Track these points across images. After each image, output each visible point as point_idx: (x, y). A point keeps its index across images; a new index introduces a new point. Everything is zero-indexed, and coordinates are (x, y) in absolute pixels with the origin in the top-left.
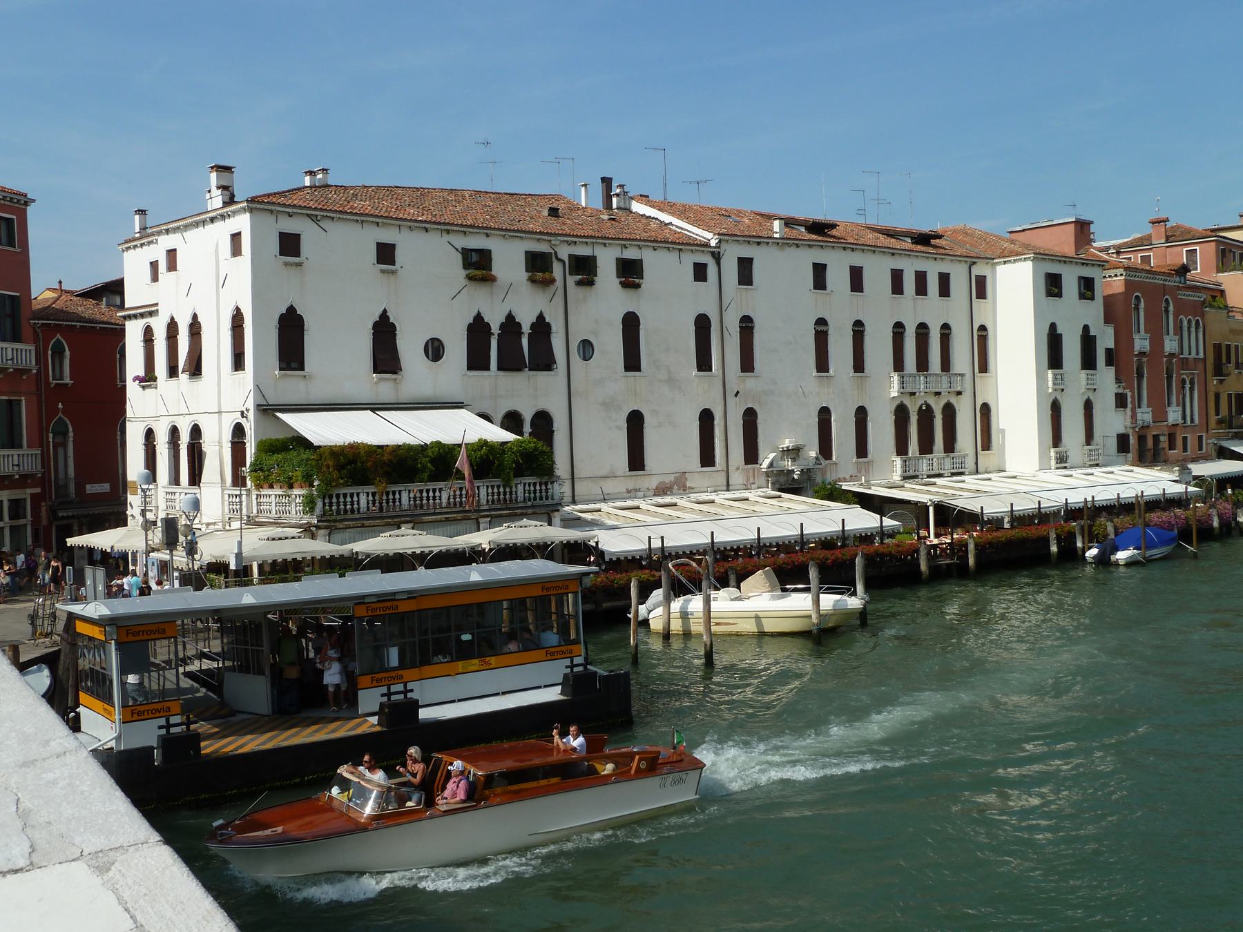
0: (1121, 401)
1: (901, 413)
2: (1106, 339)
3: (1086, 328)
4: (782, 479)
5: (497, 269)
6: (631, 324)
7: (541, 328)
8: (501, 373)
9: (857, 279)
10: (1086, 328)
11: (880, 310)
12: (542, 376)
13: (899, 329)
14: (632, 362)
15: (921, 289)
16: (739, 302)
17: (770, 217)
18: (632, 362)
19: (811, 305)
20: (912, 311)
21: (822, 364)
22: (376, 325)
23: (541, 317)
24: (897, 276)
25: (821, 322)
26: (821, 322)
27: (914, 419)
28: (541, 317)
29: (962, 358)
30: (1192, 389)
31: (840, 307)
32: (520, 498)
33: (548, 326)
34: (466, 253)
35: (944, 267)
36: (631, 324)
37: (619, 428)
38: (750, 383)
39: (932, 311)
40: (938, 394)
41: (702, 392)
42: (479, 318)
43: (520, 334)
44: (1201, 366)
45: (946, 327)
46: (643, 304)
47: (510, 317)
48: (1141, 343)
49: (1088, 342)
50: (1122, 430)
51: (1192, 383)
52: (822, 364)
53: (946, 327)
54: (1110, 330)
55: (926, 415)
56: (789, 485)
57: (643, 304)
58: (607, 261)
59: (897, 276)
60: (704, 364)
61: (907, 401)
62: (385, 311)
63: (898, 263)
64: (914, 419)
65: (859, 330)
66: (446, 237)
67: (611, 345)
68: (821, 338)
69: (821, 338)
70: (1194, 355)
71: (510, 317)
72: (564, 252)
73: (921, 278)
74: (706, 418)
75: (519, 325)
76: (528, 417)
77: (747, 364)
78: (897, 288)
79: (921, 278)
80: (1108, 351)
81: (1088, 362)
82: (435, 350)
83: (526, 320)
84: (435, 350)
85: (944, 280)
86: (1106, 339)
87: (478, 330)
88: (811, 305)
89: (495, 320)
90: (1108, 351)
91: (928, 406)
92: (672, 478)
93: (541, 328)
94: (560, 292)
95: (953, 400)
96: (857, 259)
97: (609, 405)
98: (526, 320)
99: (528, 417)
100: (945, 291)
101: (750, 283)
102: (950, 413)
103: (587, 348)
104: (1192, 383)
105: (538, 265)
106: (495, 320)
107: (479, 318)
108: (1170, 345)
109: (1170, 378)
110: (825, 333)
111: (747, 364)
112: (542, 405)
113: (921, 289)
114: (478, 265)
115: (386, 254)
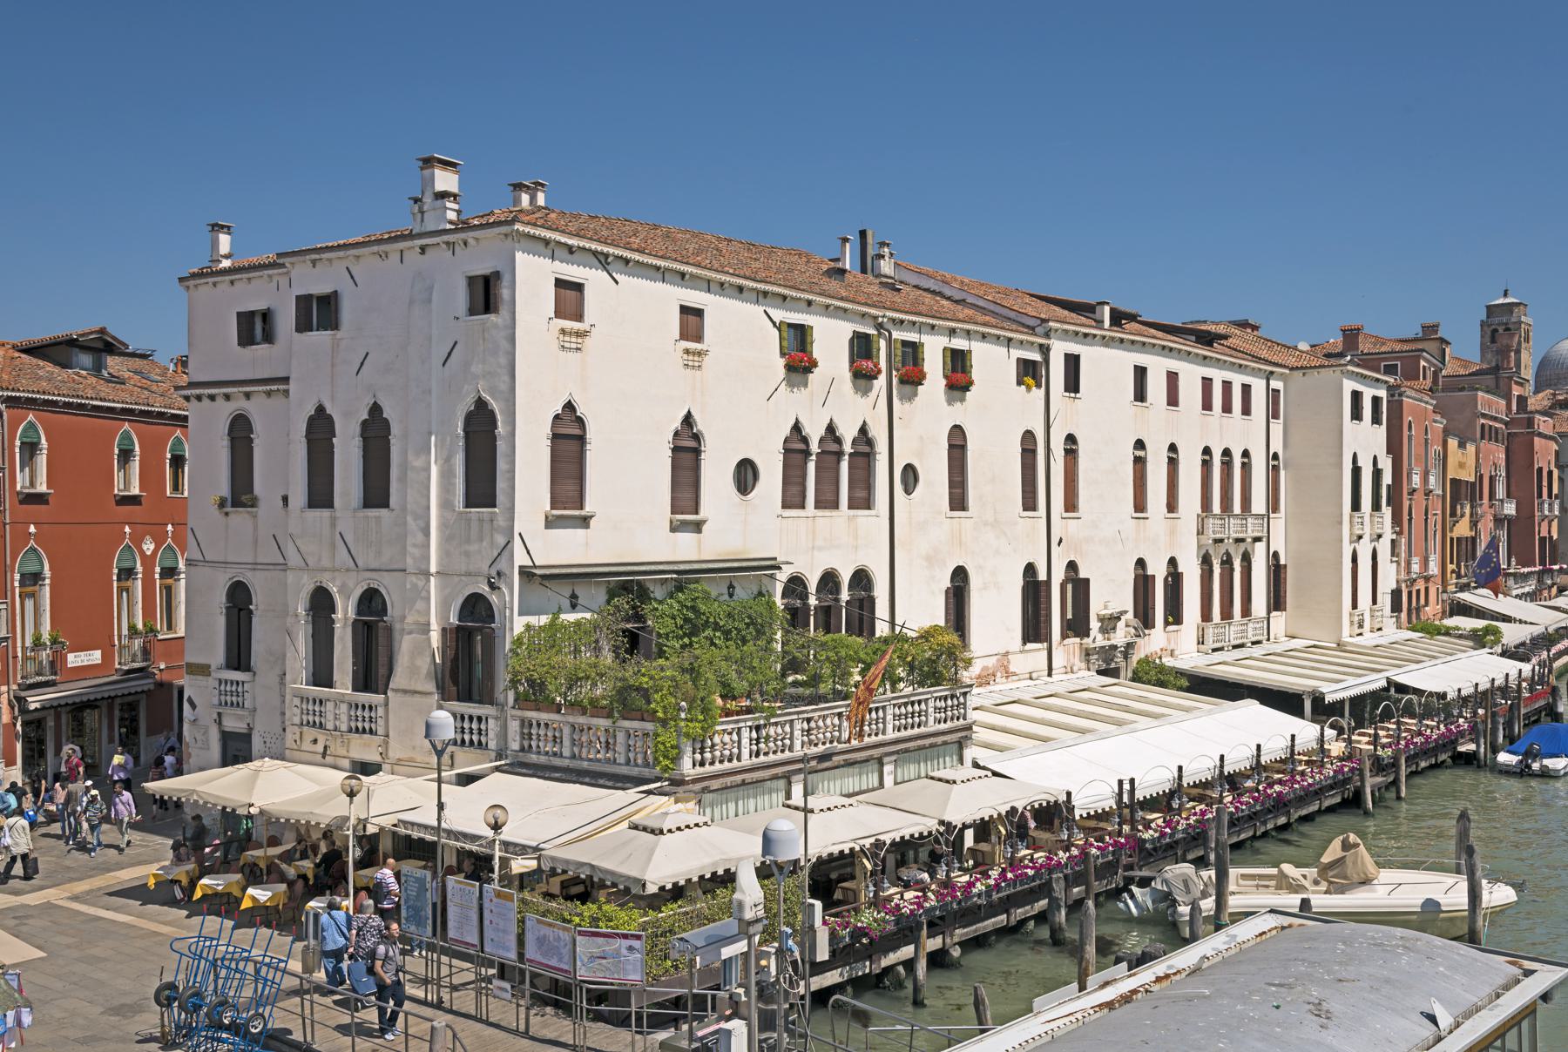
2: (1387, 479)
8: (820, 513)
14: (958, 501)
15: (1227, 408)
18: (958, 501)
21: (1140, 505)
24: (1207, 383)
25: (1140, 444)
26: (1140, 444)
28: (863, 430)
33: (870, 443)
43: (840, 454)
45: (1246, 454)
47: (831, 429)
52: (1140, 505)
53: (1246, 454)
58: (934, 349)
59: (1207, 383)
60: (1029, 503)
68: (1139, 462)
69: (1139, 462)
71: (831, 429)
73: (1227, 386)
76: (845, 577)
77: (1071, 505)
78: (1207, 405)
79: (1227, 386)
83: (848, 433)
84: (746, 475)
85: (1246, 389)
86: (1387, 479)
87: (796, 447)
98: (848, 433)
99: (845, 577)
100: (1246, 411)
101: (1077, 390)
111: (1071, 505)
113: (1227, 408)
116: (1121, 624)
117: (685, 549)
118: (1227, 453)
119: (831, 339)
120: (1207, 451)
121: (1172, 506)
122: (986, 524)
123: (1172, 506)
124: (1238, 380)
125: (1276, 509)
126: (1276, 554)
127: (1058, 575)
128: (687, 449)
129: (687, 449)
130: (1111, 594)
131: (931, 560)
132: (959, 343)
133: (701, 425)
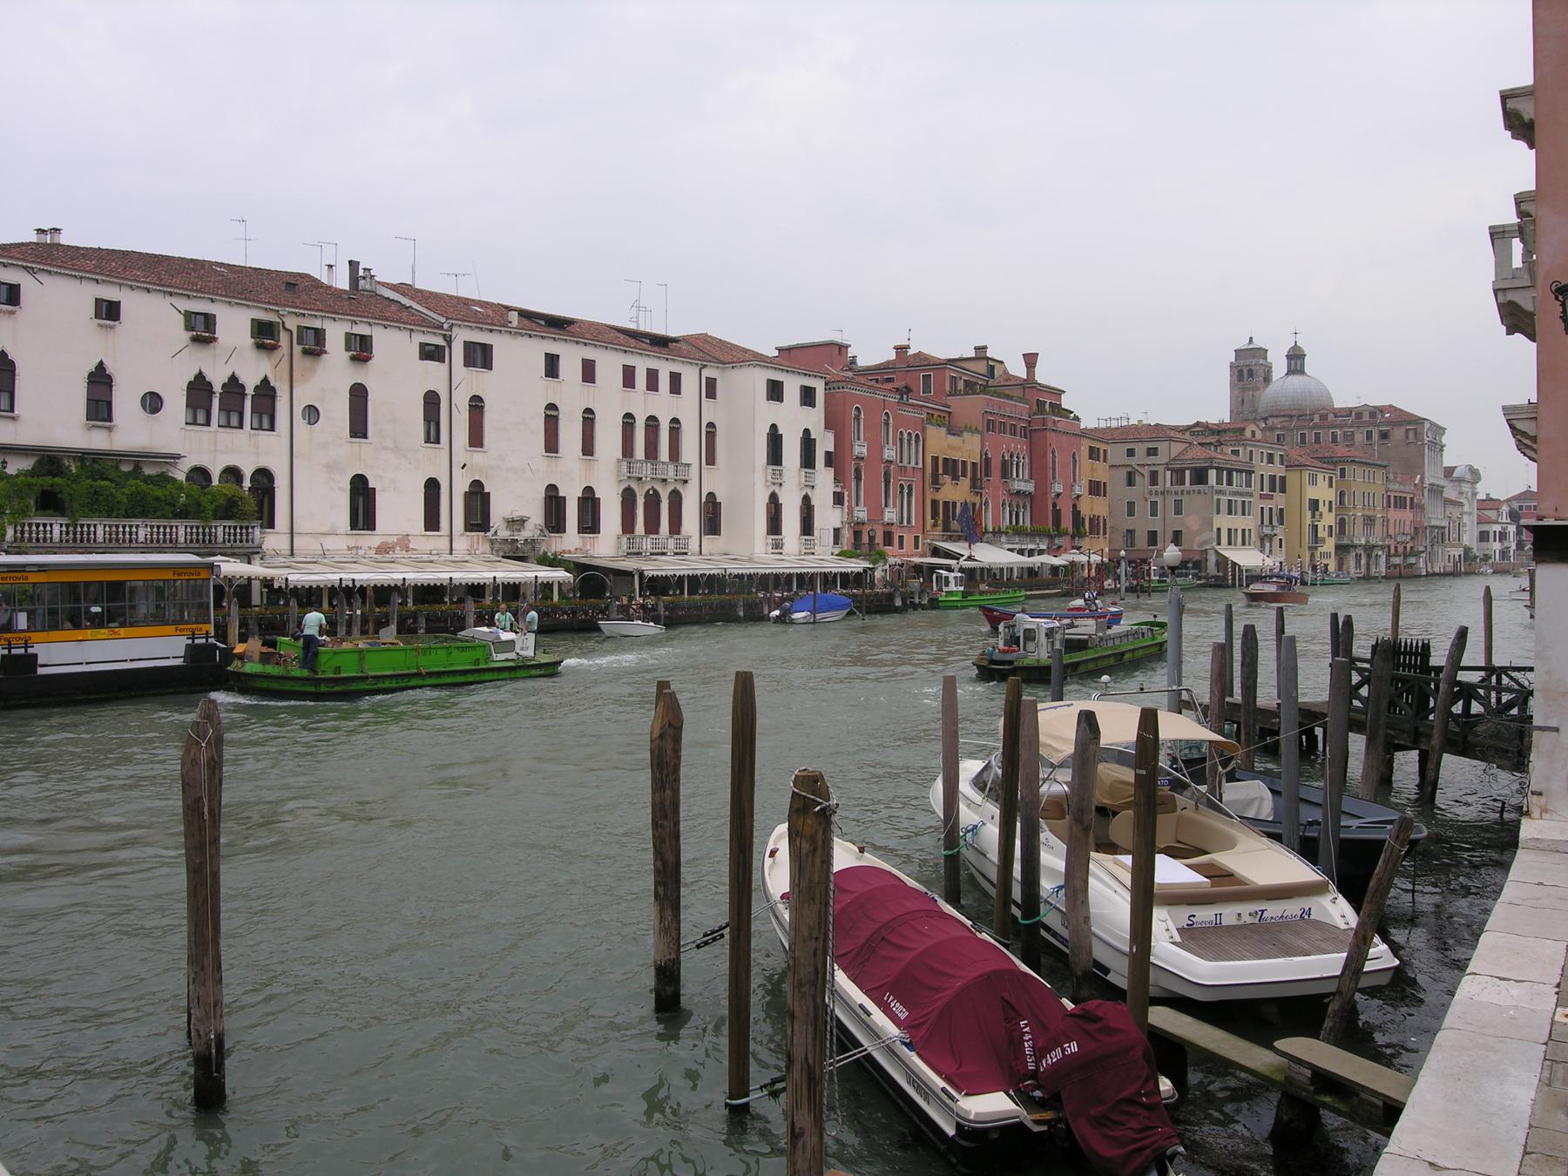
0: (838, 499)
1: (628, 498)
2: (825, 443)
3: (807, 431)
4: (507, 548)
5: (220, 331)
6: (359, 395)
7: (266, 392)
9: (589, 372)
10: (807, 431)
11: (610, 402)
12: (264, 436)
13: (628, 421)
14: (359, 428)
16: (469, 382)
17: (509, 309)
18: (359, 428)
19: (542, 391)
20: (642, 404)
21: (552, 445)
22: (91, 375)
23: (265, 381)
27: (640, 502)
28: (265, 381)
29: (691, 449)
30: (910, 495)
31: (571, 395)
32: (220, 539)
33: (273, 389)
34: (189, 317)
35: (676, 368)
36: (359, 395)
37: (341, 489)
38: (478, 457)
39: (663, 406)
40: (664, 480)
41: (433, 463)
42: (200, 377)
43: (244, 395)
44: (919, 475)
45: (675, 421)
46: (370, 376)
47: (233, 379)
48: (860, 449)
49: (808, 444)
50: (838, 525)
51: (910, 487)
52: (552, 445)
54: (830, 436)
55: (653, 500)
56: (516, 554)
57: (370, 376)
58: (336, 333)
60: (433, 437)
61: (634, 486)
62: (101, 363)
63: (630, 360)
64: (640, 502)
65: (589, 418)
66: (169, 299)
67: (338, 412)
70: (905, 463)
71: (233, 379)
72: (292, 323)
73: (652, 376)
74: (432, 486)
75: (242, 387)
76: (248, 473)
77: (476, 439)
79: (652, 376)
80: (828, 454)
81: (808, 461)
82: (153, 403)
83: (250, 382)
85: (675, 380)
87: (199, 389)
88: (542, 391)
89: (218, 380)
90: (828, 454)
91: (656, 493)
92: (395, 539)
93: (266, 392)
94: (286, 360)
95: (680, 488)
96: (590, 353)
97: (331, 468)
98: (250, 382)
99: (248, 473)
102: (676, 500)
103: (312, 413)
104: (910, 487)
105: (264, 335)
106: (218, 380)
107: (200, 377)
108: (890, 453)
109: (887, 482)
110: (556, 418)
111: (476, 439)
112: (263, 462)
113: (652, 384)
114: (202, 331)
115: (109, 311)
116: (529, 525)
117: (97, 441)
118: (652, 422)
119: (234, 323)
120: (629, 416)
121: (588, 448)
122: (385, 448)
123: (588, 448)
124: (665, 369)
125: (711, 460)
126: (711, 495)
127: (462, 486)
128: (100, 381)
129: (100, 381)
130: (516, 501)
131: (331, 468)
132: (362, 329)
133: (110, 368)
